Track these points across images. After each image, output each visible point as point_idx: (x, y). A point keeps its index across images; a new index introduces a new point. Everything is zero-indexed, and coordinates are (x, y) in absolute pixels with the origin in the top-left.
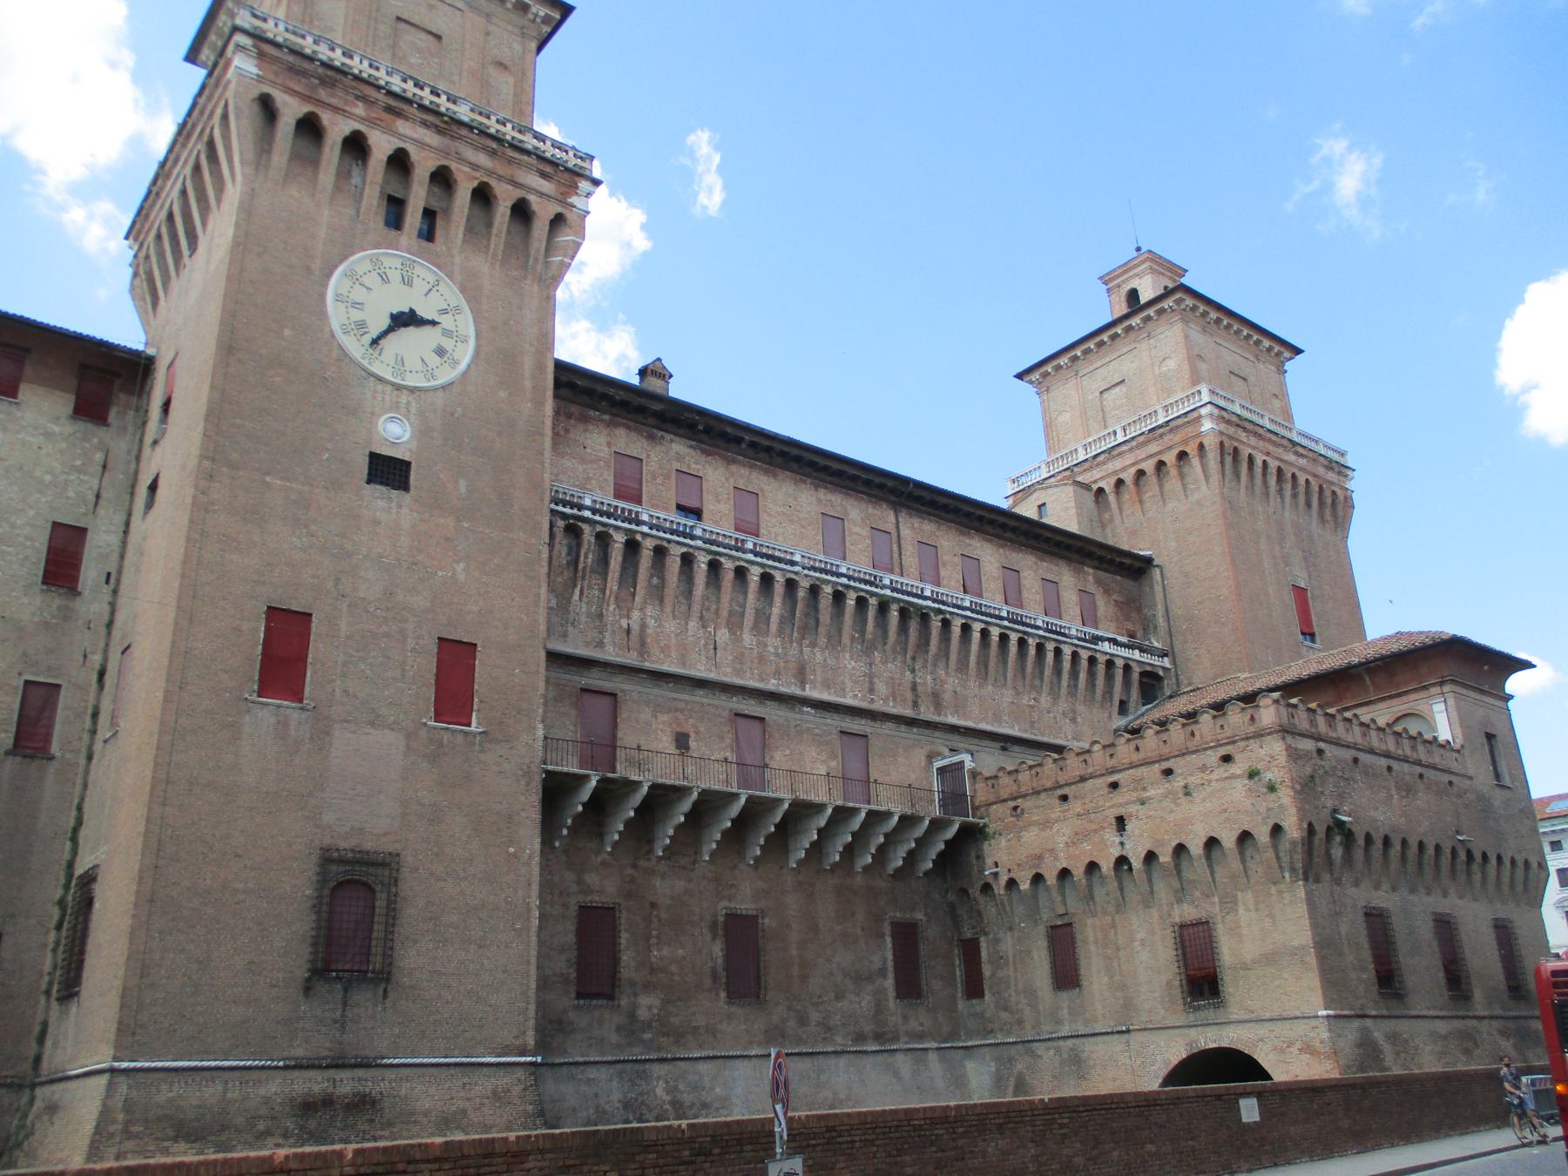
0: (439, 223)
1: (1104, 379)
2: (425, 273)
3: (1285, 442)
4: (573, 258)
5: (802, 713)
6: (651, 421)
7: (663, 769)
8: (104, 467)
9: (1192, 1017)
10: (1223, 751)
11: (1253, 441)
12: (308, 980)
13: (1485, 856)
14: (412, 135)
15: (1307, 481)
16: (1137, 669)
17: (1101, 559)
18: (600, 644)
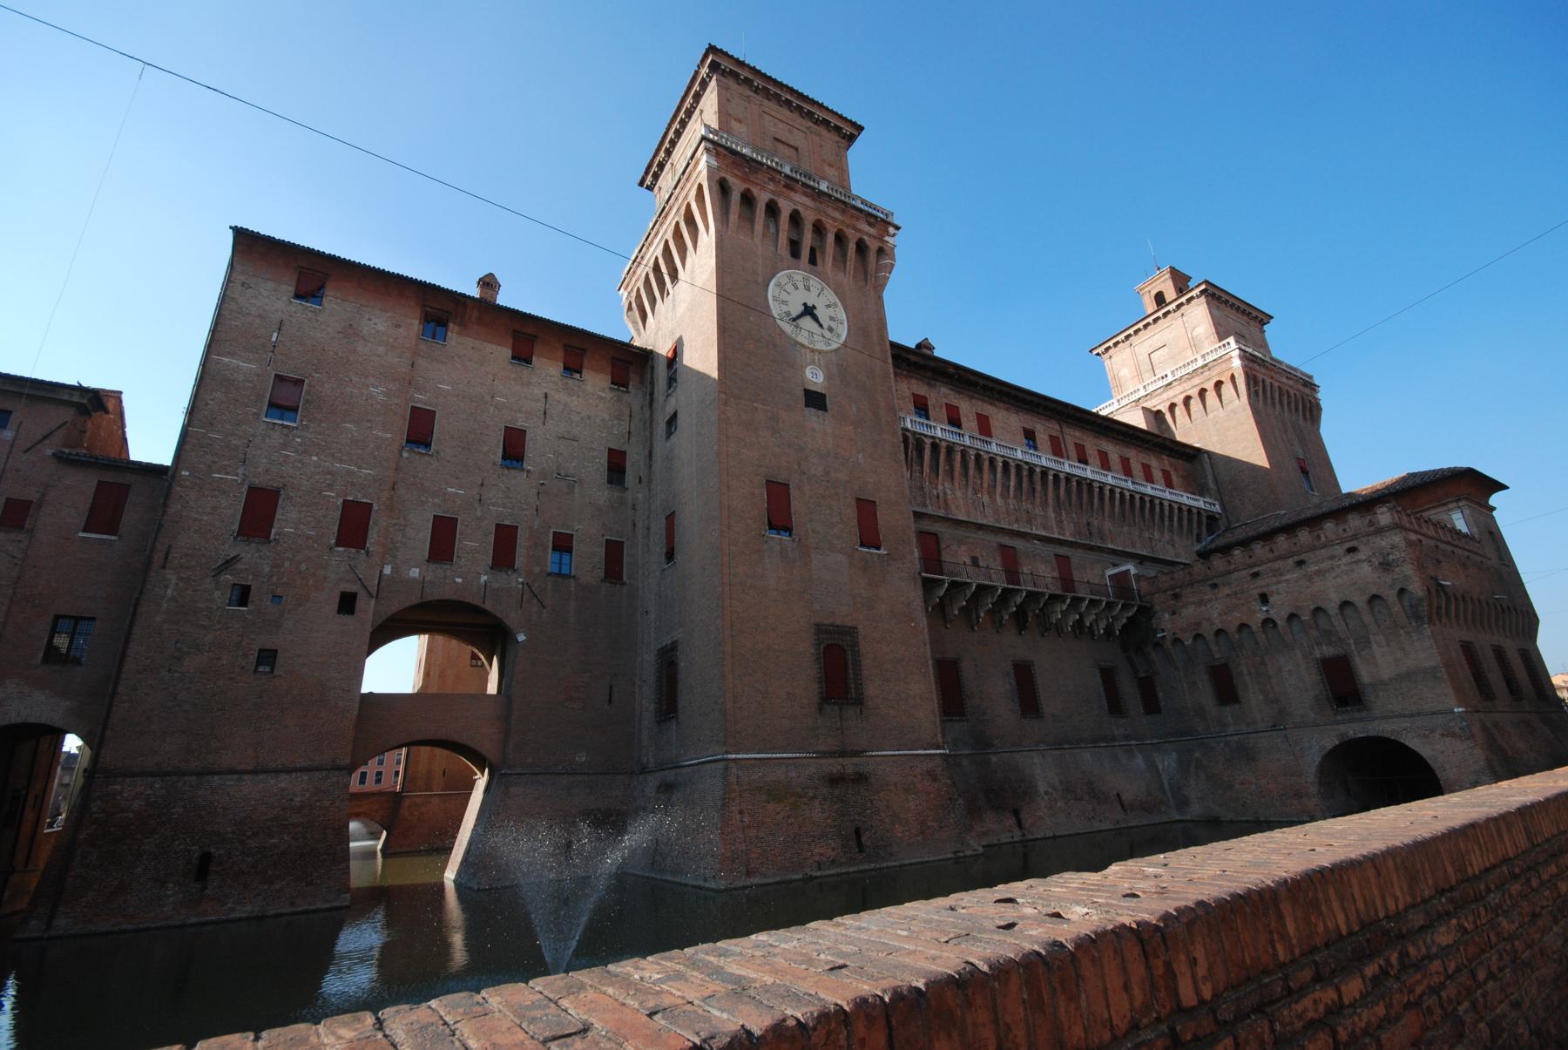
0: (818, 255)
1: (1151, 346)
2: (815, 283)
3: (1280, 370)
4: (890, 273)
6: (929, 374)
7: (974, 579)
8: (631, 416)
9: (1339, 718)
10: (1348, 545)
11: (1263, 370)
12: (820, 704)
13: (1508, 608)
14: (800, 201)
15: (1295, 394)
17: (1171, 450)
18: (925, 505)
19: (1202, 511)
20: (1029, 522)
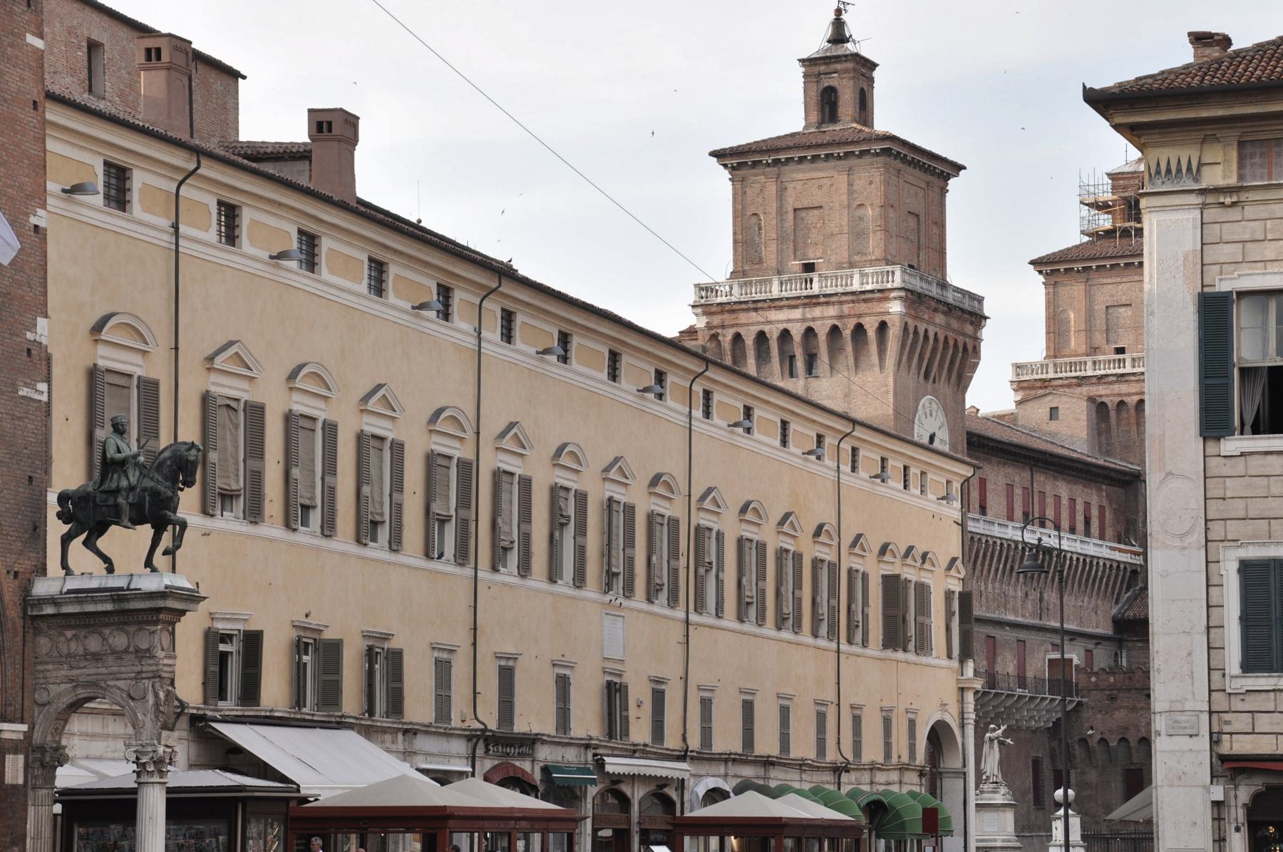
1: (1112, 296)
4: (974, 372)
5: (1006, 631)
16: (1129, 570)
19: (1128, 566)
20: (1005, 607)
